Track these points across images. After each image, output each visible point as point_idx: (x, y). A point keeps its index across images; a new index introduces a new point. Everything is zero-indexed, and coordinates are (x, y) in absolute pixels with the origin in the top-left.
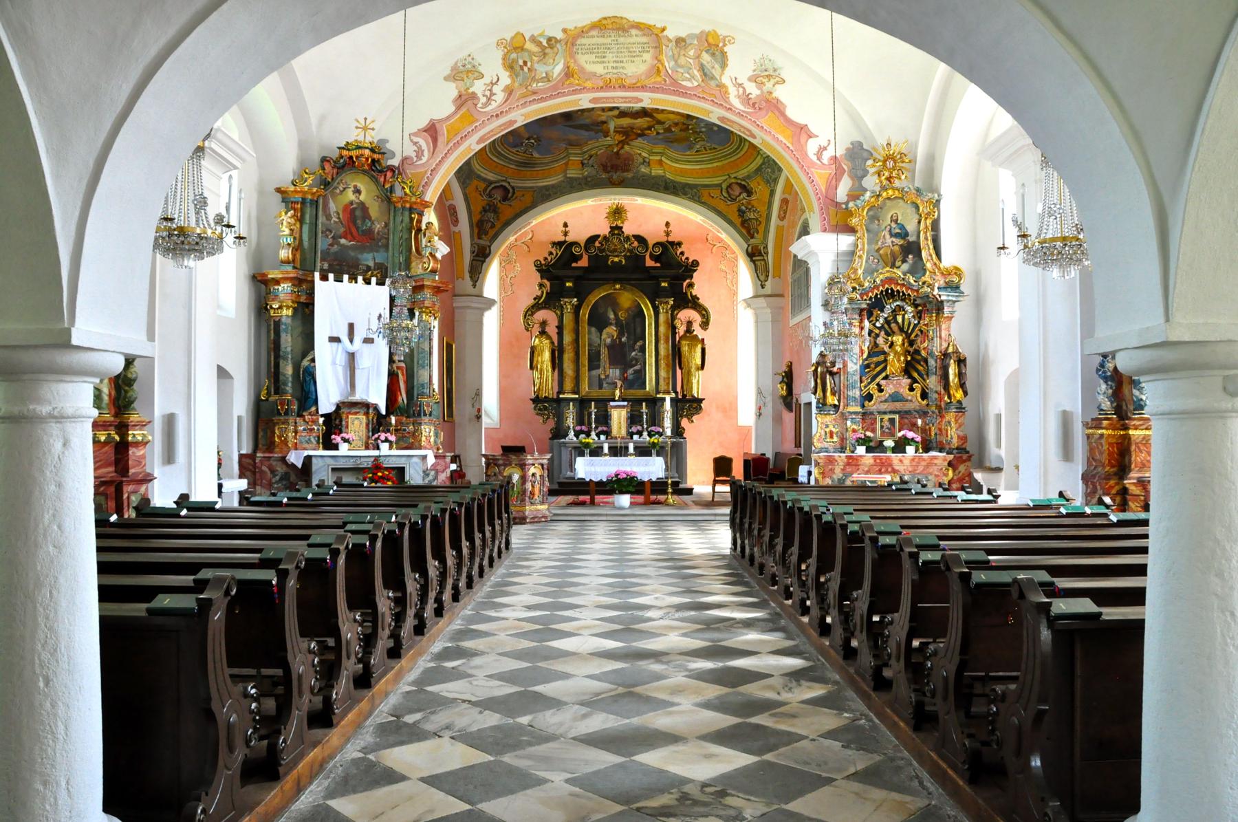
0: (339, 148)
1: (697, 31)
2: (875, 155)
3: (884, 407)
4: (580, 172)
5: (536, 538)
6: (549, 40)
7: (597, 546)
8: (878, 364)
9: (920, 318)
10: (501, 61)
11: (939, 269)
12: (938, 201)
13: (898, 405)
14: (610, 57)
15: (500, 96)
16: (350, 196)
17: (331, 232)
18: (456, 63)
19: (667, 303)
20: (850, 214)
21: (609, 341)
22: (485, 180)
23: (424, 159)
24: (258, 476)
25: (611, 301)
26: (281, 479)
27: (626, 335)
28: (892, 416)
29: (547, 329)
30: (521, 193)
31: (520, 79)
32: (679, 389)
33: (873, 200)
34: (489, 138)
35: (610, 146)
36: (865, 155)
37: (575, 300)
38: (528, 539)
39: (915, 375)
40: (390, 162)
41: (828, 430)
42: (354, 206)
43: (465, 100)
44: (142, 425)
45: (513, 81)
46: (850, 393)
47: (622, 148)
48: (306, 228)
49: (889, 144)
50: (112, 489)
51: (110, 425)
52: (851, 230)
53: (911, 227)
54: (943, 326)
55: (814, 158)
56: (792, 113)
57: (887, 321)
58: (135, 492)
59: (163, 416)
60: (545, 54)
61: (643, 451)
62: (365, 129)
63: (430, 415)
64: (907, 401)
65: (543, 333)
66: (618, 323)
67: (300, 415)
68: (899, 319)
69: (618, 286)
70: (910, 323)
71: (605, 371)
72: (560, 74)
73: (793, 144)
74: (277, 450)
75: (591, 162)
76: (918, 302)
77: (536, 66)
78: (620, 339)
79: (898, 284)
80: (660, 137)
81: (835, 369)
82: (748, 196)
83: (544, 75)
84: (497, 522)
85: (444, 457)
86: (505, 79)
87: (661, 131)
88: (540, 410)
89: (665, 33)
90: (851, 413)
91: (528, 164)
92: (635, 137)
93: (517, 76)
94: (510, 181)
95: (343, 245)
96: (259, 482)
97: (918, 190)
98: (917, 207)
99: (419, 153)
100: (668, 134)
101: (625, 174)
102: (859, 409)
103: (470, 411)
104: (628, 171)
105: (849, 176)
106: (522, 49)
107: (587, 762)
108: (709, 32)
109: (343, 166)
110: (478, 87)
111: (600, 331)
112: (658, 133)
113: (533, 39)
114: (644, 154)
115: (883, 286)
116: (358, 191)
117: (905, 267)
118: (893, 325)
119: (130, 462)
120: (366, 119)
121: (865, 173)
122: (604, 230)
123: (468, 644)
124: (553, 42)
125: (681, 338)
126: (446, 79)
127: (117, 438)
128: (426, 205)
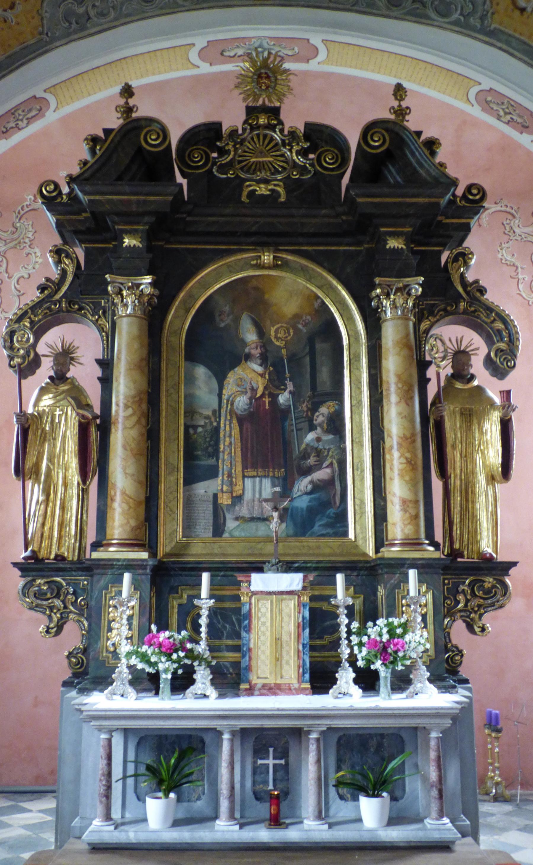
19: (405, 290)
27: (290, 386)
32: (439, 537)
37: (148, 279)
69: (267, 258)
71: (231, 484)
78: (274, 397)
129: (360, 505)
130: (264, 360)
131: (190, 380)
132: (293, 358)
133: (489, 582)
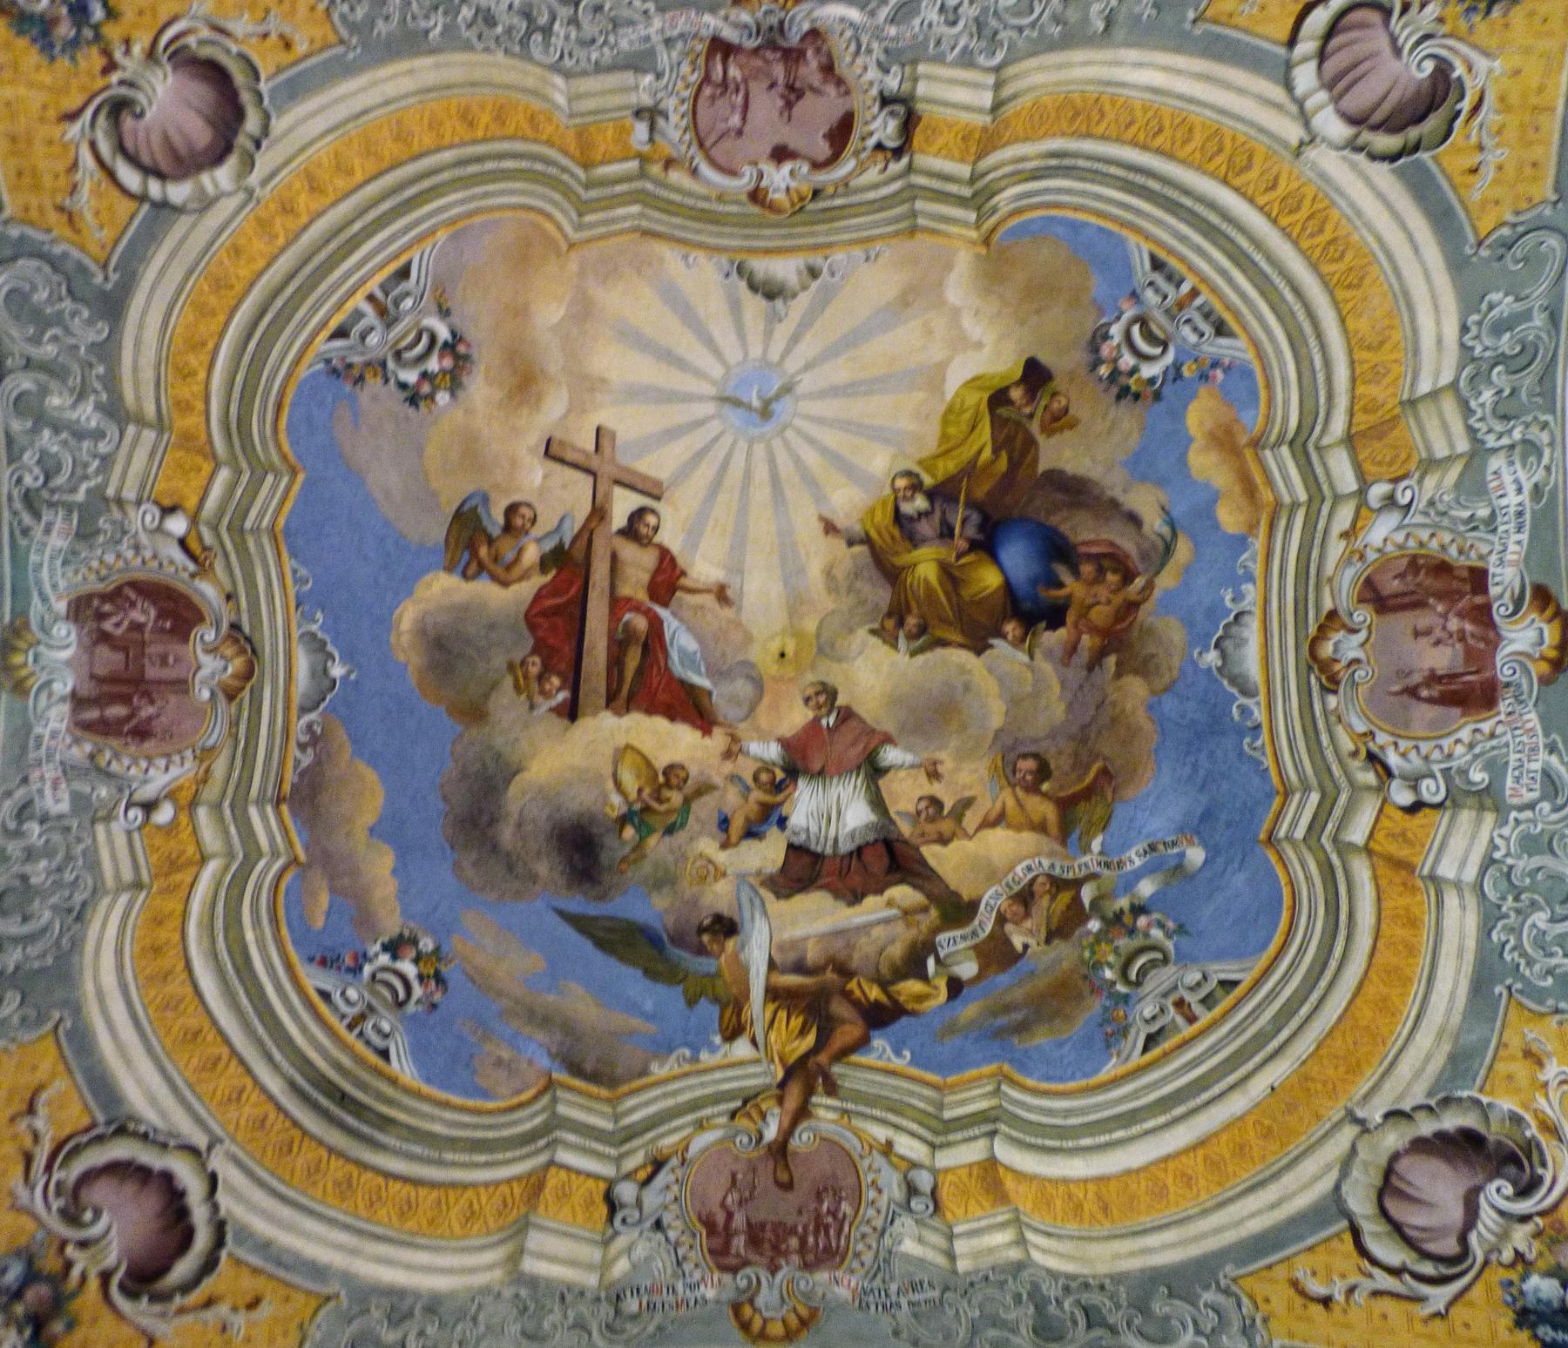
4: (596, 1254)
22: (102, 1087)
30: (248, 1284)
47: (803, 1112)
75: (652, 1198)
80: (969, 1010)
82: (1524, 1192)
87: (967, 969)
91: (358, 1109)
94: (217, 1162)
100: (1003, 979)
101: (822, 1276)
112: (956, 987)
114: (908, 1147)
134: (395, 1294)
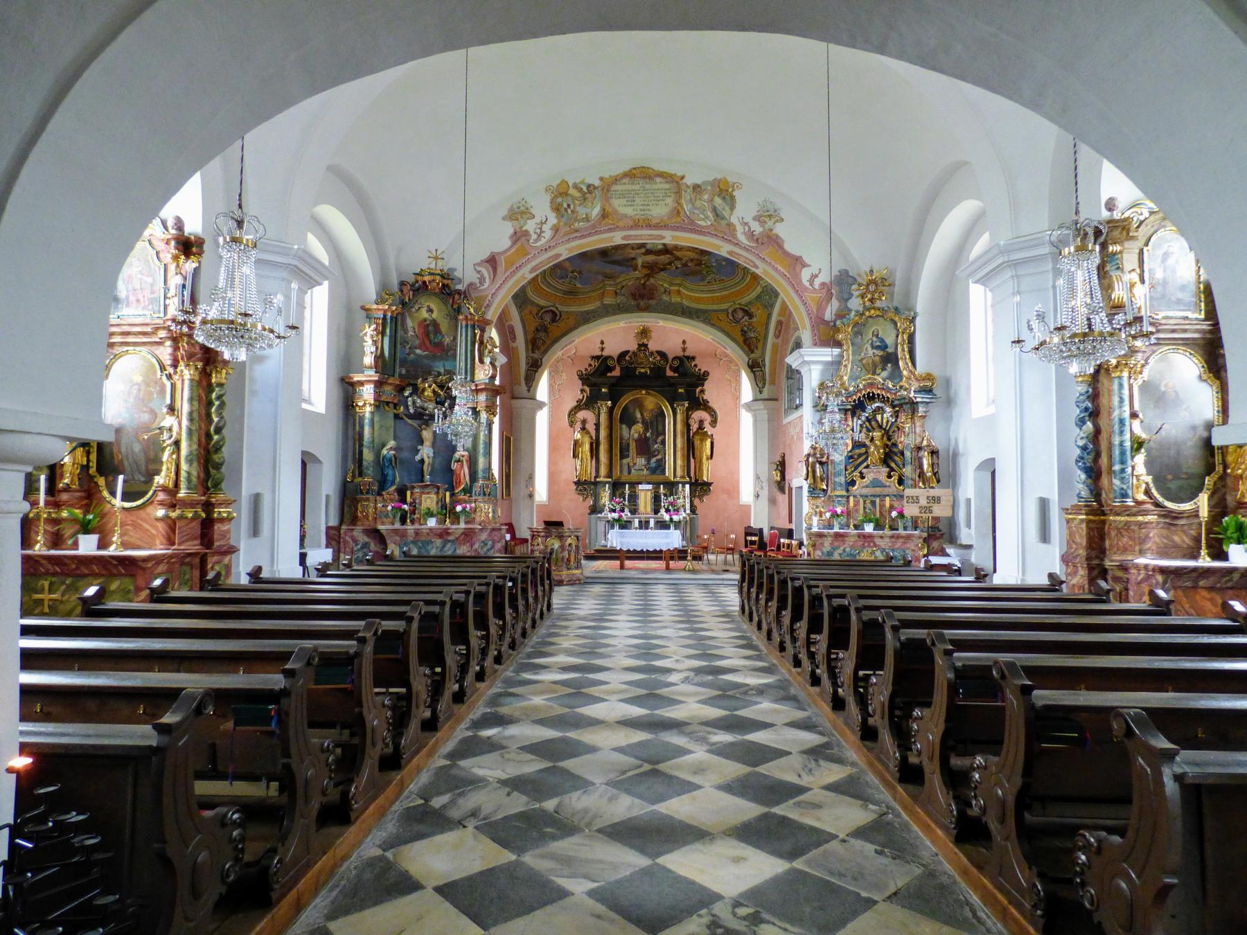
0: (415, 274)
1: (711, 179)
2: (859, 280)
3: (865, 491)
5: (575, 599)
6: (589, 186)
7: (625, 607)
8: (860, 455)
9: (897, 417)
10: (549, 204)
11: (914, 375)
12: (914, 318)
13: (878, 491)
14: (638, 200)
15: (548, 234)
16: (424, 314)
17: (408, 344)
18: (512, 206)
19: (683, 405)
20: (838, 331)
21: (636, 436)
22: (537, 305)
23: (486, 285)
24: (342, 545)
25: (639, 404)
26: (362, 547)
27: (650, 431)
28: (873, 499)
29: (587, 426)
31: (564, 220)
32: (692, 475)
33: (857, 318)
34: (539, 269)
35: (638, 278)
36: (850, 281)
37: (610, 402)
38: (568, 600)
39: (893, 465)
40: (459, 287)
41: (818, 510)
42: (428, 322)
43: (519, 236)
44: (227, 503)
45: (559, 221)
46: (837, 480)
47: (648, 279)
48: (386, 340)
49: (872, 271)
50: (197, 560)
51: (198, 504)
52: (838, 344)
53: (890, 340)
54: (918, 424)
55: (807, 284)
56: (789, 247)
57: (868, 420)
58: (219, 562)
59: (250, 496)
60: (585, 199)
61: (662, 525)
62: (436, 258)
63: (489, 495)
64: (885, 486)
65: (583, 429)
66: (644, 422)
67: (379, 494)
68: (879, 417)
69: (644, 392)
70: (888, 421)
72: (597, 215)
73: (789, 273)
74: (359, 523)
75: (623, 291)
76: (896, 402)
77: (578, 208)
79: (878, 388)
80: (678, 271)
81: (824, 460)
83: (584, 216)
84: (540, 588)
85: (500, 529)
86: (553, 220)
87: (680, 266)
88: (581, 490)
89: (684, 181)
90: (838, 496)
92: (657, 271)
93: (562, 216)
95: (418, 355)
96: (342, 550)
97: (896, 309)
98: (895, 324)
99: (482, 280)
100: (686, 268)
102: (844, 493)
103: (525, 492)
104: (652, 298)
105: (837, 299)
106: (567, 194)
107: (615, 867)
108: (721, 179)
109: (418, 289)
110: (530, 226)
111: (630, 429)
112: (677, 268)
113: (576, 186)
114: (666, 285)
115: (866, 390)
116: (430, 310)
117: (885, 374)
118: (873, 423)
119: (215, 536)
120: (436, 250)
121: (851, 296)
122: (633, 346)
123: (504, 710)
124: (591, 188)
125: (694, 434)
126: (504, 219)
127: (204, 515)
128: (488, 323)
129: (669, 468)
130: (643, 423)
131: (621, 429)
132: (651, 423)
133: (705, 488)
134: (585, 311)
